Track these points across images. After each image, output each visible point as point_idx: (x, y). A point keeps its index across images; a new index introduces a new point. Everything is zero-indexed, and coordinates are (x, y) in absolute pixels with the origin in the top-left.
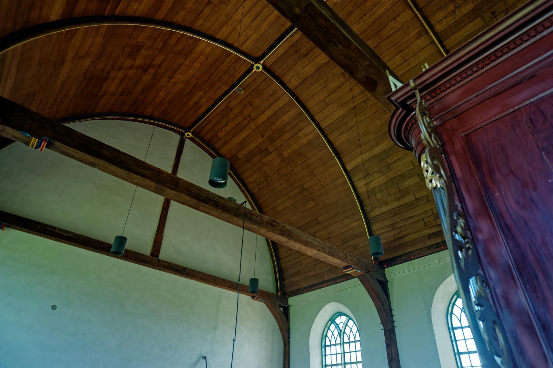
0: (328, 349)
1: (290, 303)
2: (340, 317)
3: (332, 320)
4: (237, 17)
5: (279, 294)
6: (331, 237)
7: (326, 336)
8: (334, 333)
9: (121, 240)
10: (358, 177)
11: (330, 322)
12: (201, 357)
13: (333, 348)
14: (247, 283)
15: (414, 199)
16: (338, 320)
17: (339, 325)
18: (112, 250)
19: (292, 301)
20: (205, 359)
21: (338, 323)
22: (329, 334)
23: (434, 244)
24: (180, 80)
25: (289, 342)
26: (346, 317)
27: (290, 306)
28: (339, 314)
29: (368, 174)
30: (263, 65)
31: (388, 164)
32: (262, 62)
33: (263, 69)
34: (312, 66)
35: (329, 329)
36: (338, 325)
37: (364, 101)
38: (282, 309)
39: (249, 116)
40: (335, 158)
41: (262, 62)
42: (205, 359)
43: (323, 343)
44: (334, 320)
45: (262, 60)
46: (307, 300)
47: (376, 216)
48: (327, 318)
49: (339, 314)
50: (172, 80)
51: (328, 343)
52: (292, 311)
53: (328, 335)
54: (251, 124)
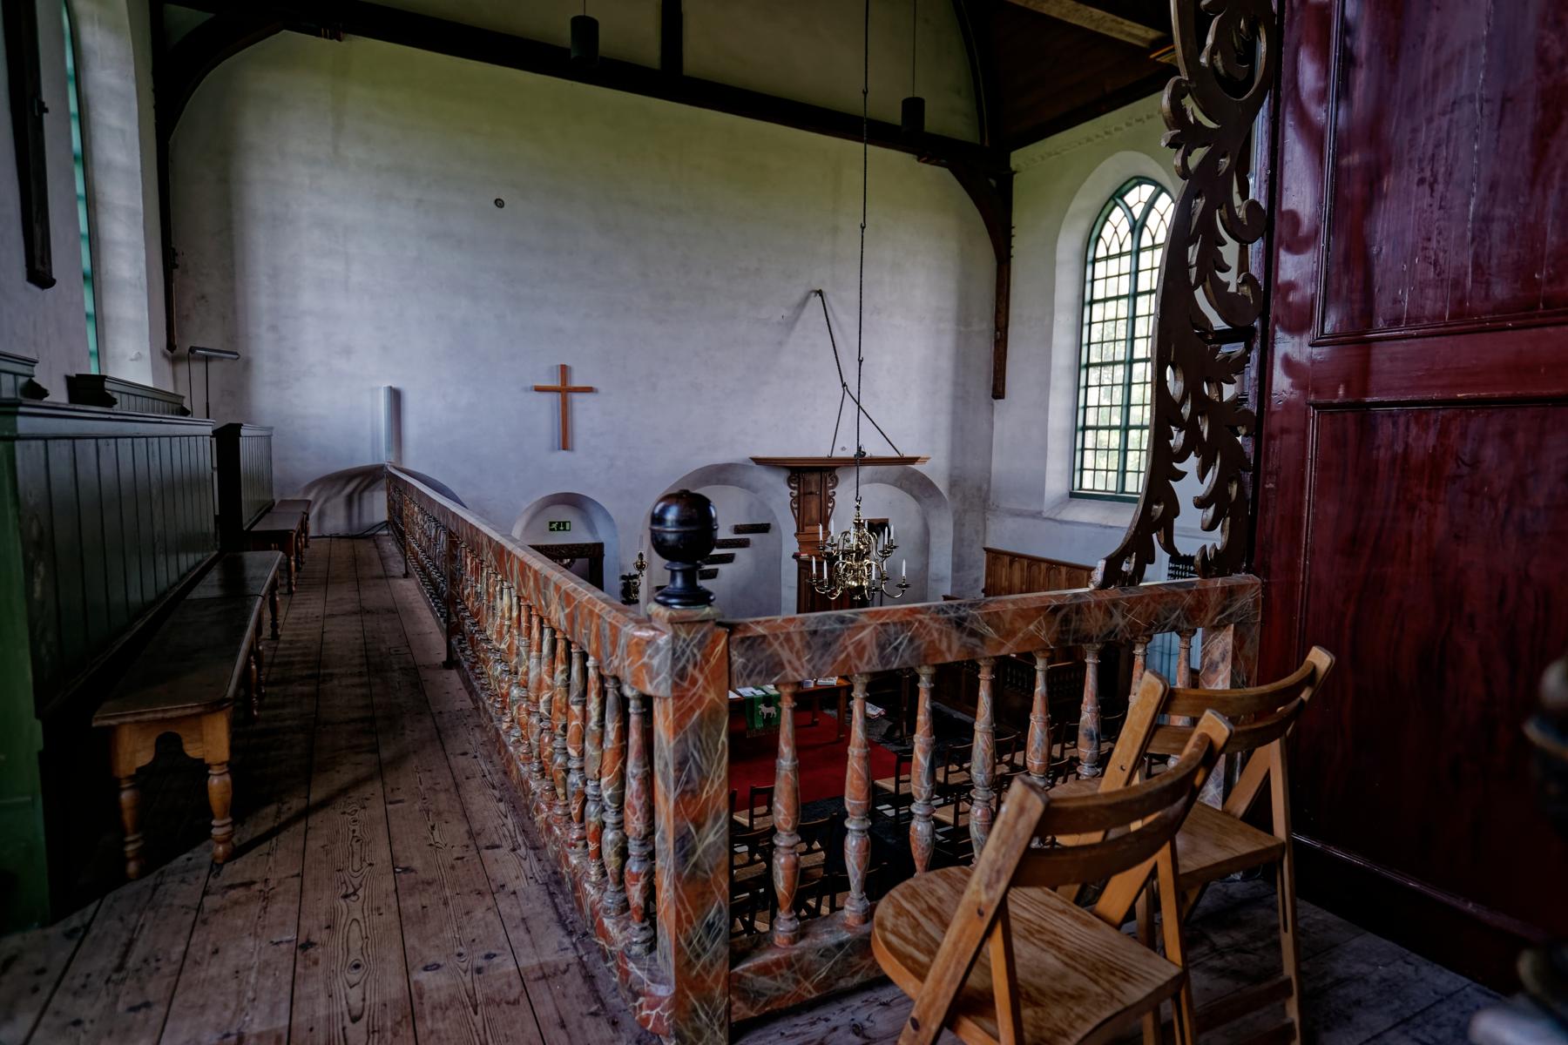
0: (1100, 266)
1: (1013, 166)
2: (1138, 188)
3: (1118, 195)
5: (987, 144)
7: (1099, 237)
8: (1118, 230)
9: (585, 28)
11: (1112, 203)
12: (812, 292)
13: (1113, 263)
14: (895, 116)
16: (1130, 198)
17: (1133, 210)
18: (573, 55)
19: (1018, 158)
20: (821, 295)
21: (1130, 205)
22: (1107, 232)
25: (1009, 257)
26: (1153, 188)
27: (1015, 172)
28: (1134, 181)
35: (1107, 219)
36: (1130, 209)
38: (993, 182)
42: (821, 295)
43: (1090, 255)
44: (1122, 197)
46: (1057, 153)
48: (1108, 190)
49: (1134, 181)
51: (1101, 253)
52: (1018, 183)
53: (1103, 234)
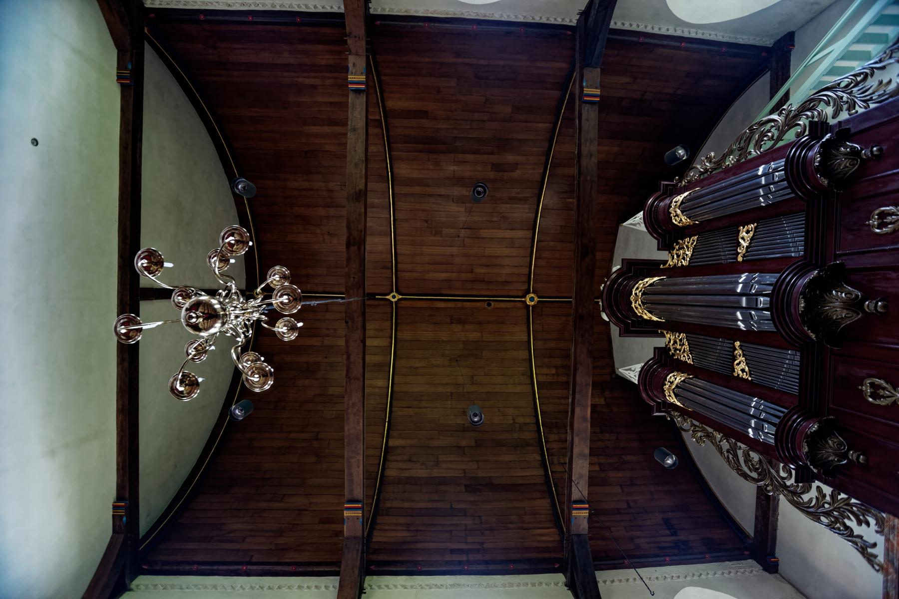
4: (425, 250)
6: (307, 510)
10: (395, 458)
15: (449, 507)
23: (456, 561)
24: (331, 243)
29: (410, 460)
30: (399, 300)
31: (438, 461)
32: (401, 297)
33: (396, 302)
34: (432, 335)
37: (452, 393)
39: (335, 330)
40: (387, 423)
41: (401, 297)
45: (402, 296)
47: (390, 508)
50: (326, 237)
54: (328, 338)
